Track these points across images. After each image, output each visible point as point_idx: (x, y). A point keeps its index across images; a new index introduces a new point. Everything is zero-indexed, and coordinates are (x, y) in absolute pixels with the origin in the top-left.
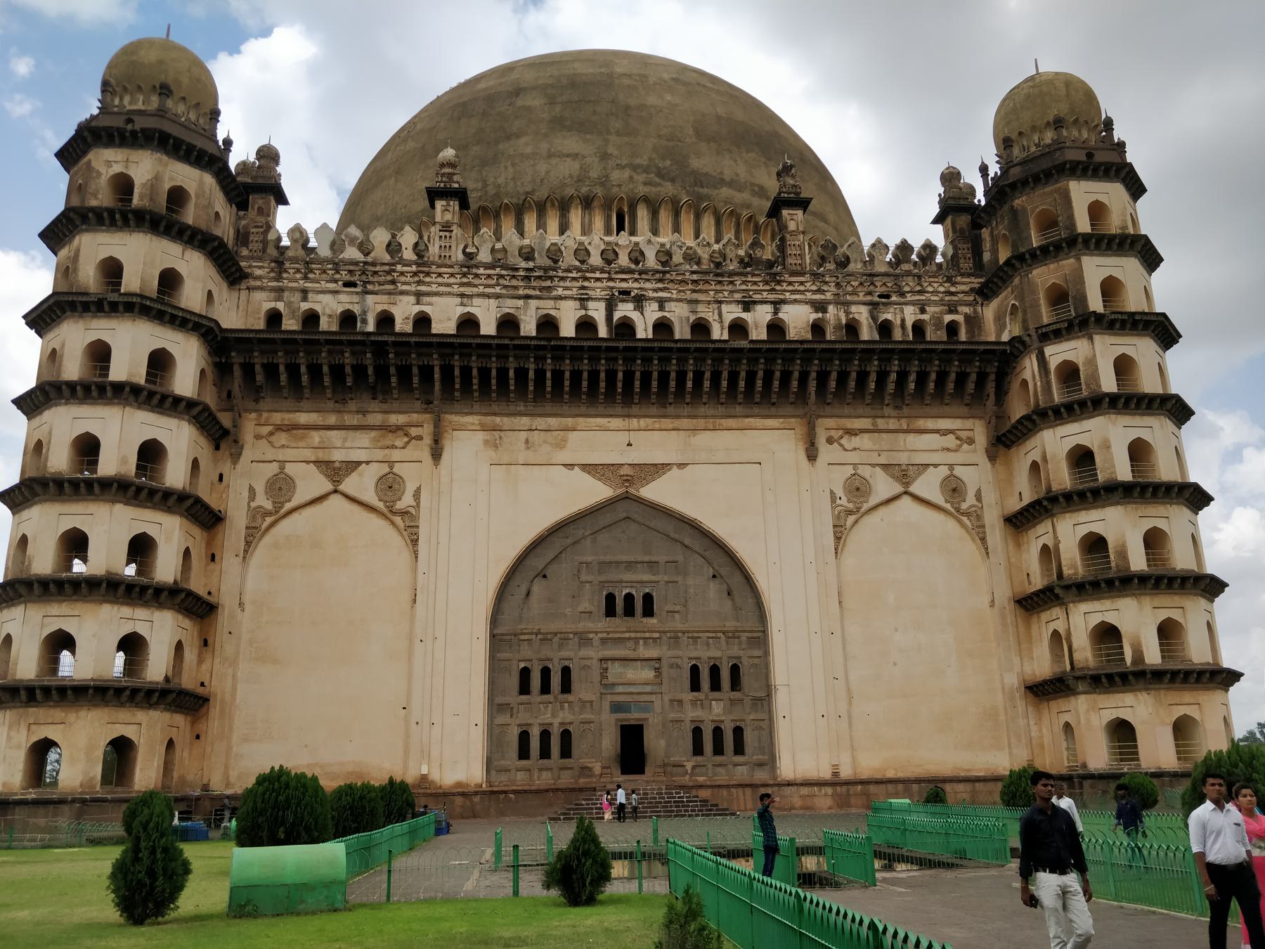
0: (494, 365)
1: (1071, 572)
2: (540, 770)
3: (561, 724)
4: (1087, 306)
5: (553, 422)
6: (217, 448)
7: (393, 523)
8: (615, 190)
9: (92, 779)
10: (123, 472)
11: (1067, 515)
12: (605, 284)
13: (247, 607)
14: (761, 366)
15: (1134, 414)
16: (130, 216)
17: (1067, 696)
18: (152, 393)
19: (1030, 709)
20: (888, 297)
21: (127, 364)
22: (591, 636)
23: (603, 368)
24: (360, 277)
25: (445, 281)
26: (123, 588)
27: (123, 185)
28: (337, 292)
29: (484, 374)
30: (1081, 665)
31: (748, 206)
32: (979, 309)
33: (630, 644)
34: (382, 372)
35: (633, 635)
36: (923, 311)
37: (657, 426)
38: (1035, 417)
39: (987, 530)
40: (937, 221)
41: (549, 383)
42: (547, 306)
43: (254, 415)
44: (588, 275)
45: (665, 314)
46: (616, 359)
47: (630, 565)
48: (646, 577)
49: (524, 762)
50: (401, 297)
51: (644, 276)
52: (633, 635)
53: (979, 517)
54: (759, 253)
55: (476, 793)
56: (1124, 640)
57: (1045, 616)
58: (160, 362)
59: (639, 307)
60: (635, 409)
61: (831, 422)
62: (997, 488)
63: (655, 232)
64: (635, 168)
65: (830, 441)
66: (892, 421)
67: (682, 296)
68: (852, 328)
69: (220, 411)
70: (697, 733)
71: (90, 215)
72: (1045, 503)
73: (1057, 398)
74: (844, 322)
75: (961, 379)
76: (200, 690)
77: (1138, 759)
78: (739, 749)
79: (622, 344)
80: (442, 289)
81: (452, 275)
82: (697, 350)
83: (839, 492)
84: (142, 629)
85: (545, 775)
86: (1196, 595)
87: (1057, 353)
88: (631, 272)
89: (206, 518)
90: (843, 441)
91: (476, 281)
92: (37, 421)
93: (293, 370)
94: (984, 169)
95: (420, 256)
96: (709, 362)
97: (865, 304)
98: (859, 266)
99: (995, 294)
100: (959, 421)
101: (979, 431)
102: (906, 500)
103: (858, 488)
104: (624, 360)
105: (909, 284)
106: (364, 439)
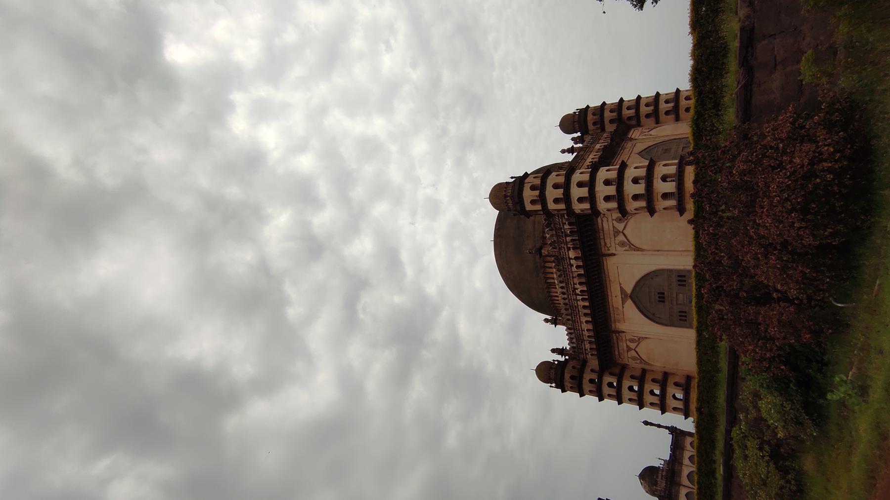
61: (603, 249)
89: (644, 371)
102: (625, 232)
103: (622, 244)
106: (621, 344)
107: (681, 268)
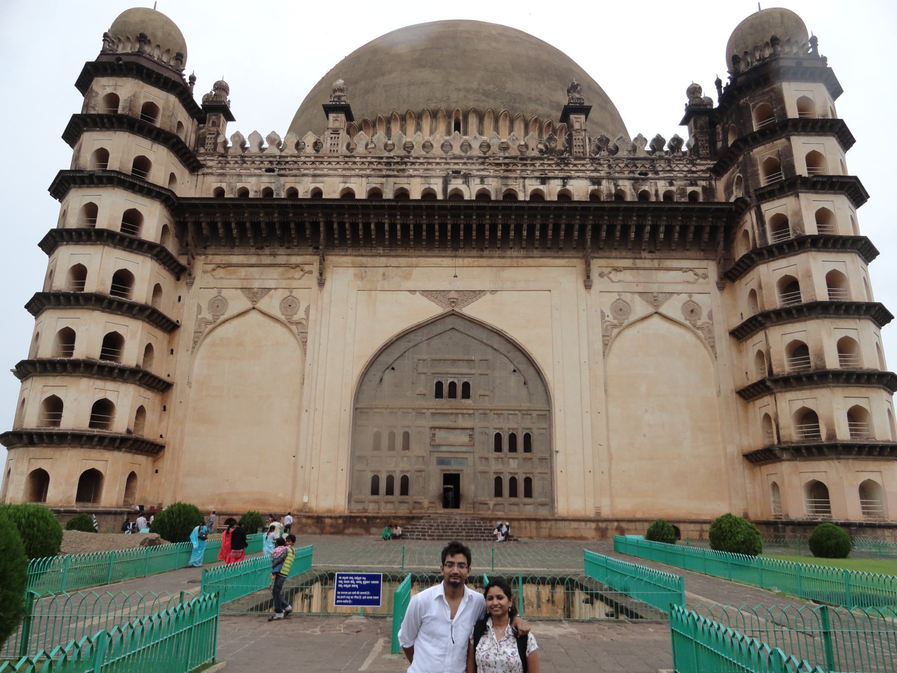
0: (360, 221)
1: (779, 370)
2: (386, 502)
3: (402, 471)
4: (794, 172)
5: (403, 261)
6: (178, 279)
7: (291, 330)
8: (453, 106)
9: (70, 497)
10: (101, 290)
11: (777, 327)
12: (443, 166)
13: (193, 384)
14: (551, 221)
15: (831, 252)
16: (114, 120)
17: (774, 462)
18: (127, 236)
19: (746, 472)
20: (646, 174)
21: (110, 218)
22: (424, 411)
23: (437, 222)
24: (276, 164)
25: (334, 166)
26: (96, 368)
27: (113, 100)
28: (261, 175)
29: (354, 226)
30: (786, 440)
31: (548, 116)
32: (713, 182)
33: (452, 418)
34: (285, 226)
35: (454, 411)
36: (671, 184)
37: (476, 264)
38: (753, 256)
39: (716, 340)
40: (684, 123)
41: (399, 233)
42: (403, 183)
43: (203, 257)
44: (431, 161)
45: (485, 186)
46: (446, 216)
47: (454, 361)
48: (465, 371)
49: (375, 497)
50: (303, 178)
51: (471, 161)
52: (454, 411)
53: (710, 331)
54: (553, 145)
55: (340, 517)
56: (820, 421)
57: (759, 403)
58: (132, 219)
59: (466, 182)
60: (461, 252)
62: (725, 309)
63: (481, 133)
64: (467, 90)
65: (601, 275)
66: (647, 261)
67: (497, 174)
68: (619, 195)
69: (180, 254)
70: (498, 481)
71: (88, 120)
72: (760, 319)
73: (771, 241)
74: (613, 191)
75: (699, 230)
76: (160, 441)
77: (830, 512)
78: (528, 493)
79: (449, 204)
80: (331, 172)
81: (338, 163)
82: (504, 208)
83: (607, 312)
84: (111, 397)
85: (389, 506)
86: (879, 388)
87: (770, 209)
88: (461, 158)
89: (170, 327)
90: (611, 276)
91: (354, 167)
92: (52, 257)
93: (227, 226)
94: (718, 83)
95: (317, 151)
96: (513, 217)
97: (629, 179)
98: (625, 153)
99: (725, 171)
100: (696, 262)
101: (711, 269)
102: (656, 319)
103: (621, 309)
104: (452, 216)
105: (661, 165)
106: (275, 273)
107: (559, 443)
